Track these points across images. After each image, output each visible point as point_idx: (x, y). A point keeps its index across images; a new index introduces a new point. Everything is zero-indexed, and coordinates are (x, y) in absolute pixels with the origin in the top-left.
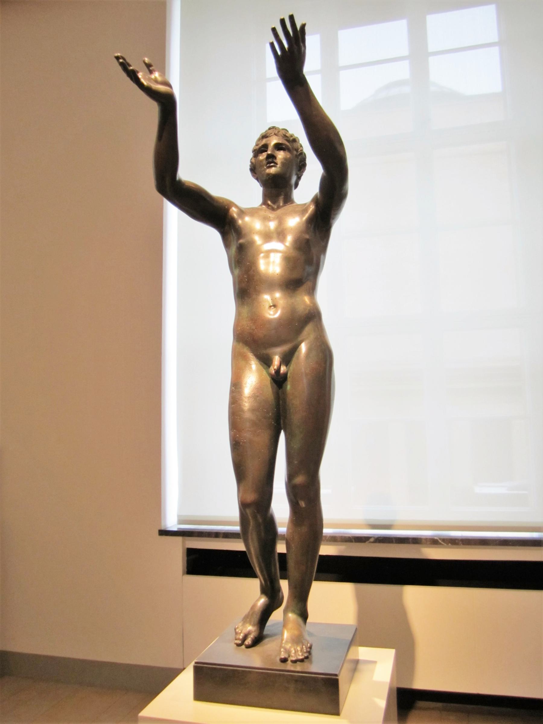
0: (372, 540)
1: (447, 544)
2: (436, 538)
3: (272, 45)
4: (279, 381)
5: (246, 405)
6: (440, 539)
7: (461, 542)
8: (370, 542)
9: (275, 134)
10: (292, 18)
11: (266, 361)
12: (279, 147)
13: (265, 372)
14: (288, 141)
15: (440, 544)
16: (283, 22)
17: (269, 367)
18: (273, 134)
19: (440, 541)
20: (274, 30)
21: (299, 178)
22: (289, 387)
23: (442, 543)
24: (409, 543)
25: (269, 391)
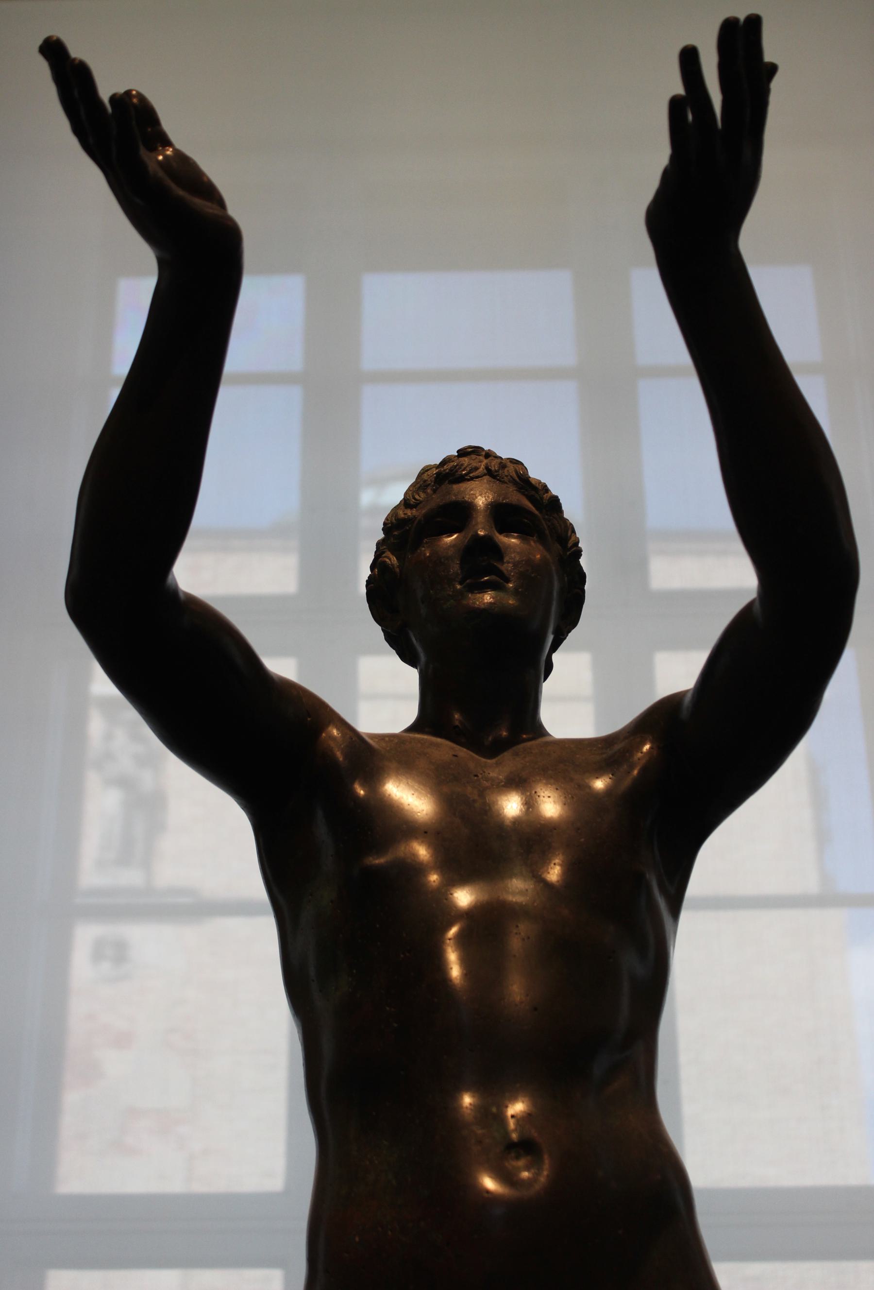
3: (676, 106)
9: (489, 472)
10: (754, 23)
12: (504, 516)
20: (689, 59)
21: (555, 647)
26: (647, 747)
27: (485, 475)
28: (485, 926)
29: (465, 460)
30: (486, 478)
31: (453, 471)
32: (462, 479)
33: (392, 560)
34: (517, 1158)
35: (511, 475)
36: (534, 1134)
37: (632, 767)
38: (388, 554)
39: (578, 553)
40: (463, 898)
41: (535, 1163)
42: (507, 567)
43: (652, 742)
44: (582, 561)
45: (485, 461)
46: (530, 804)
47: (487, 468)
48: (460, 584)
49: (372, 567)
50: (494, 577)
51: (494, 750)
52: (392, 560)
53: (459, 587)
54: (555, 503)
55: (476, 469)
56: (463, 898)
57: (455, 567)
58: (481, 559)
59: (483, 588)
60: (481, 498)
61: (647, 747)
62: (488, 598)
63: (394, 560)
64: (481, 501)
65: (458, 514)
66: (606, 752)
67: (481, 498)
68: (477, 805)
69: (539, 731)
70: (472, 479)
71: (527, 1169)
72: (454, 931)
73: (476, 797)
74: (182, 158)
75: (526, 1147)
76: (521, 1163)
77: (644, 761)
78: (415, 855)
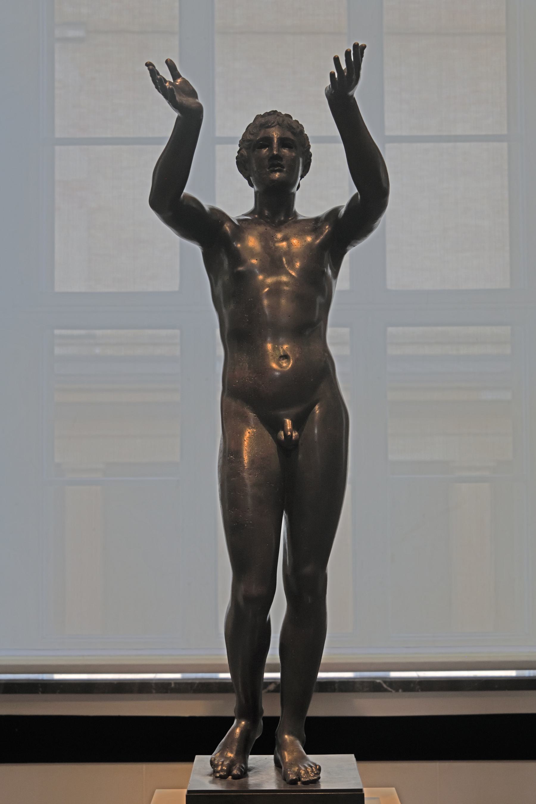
0: (272, 687)
1: (397, 691)
2: (378, 681)
3: (332, 75)
4: (287, 449)
5: (248, 477)
6: (385, 682)
7: (418, 687)
8: (269, 691)
9: (278, 124)
11: (273, 425)
12: (284, 143)
13: (269, 438)
14: (294, 133)
15: (385, 690)
16: (348, 53)
17: (278, 431)
19: (385, 686)
20: (336, 60)
22: (300, 456)
23: (389, 689)
24: (333, 690)
26: (327, 227)
28: (276, 291)
30: (277, 126)
31: (266, 123)
32: (269, 127)
33: (244, 152)
36: (288, 353)
37: (322, 234)
38: (243, 150)
40: (269, 280)
41: (289, 361)
42: (284, 162)
43: (329, 226)
44: (311, 150)
45: (278, 118)
46: (290, 245)
48: (268, 169)
49: (238, 152)
50: (280, 168)
51: (279, 226)
52: (244, 152)
53: (268, 170)
55: (273, 123)
56: (269, 280)
57: (266, 162)
58: (275, 162)
59: (276, 171)
60: (275, 134)
62: (277, 175)
63: (245, 152)
64: (275, 136)
65: (267, 142)
66: (315, 225)
67: (275, 134)
68: (273, 248)
69: (295, 214)
70: (272, 127)
71: (285, 363)
72: (266, 290)
73: (272, 246)
74: (185, 82)
75: (285, 357)
76: (284, 361)
78: (252, 264)
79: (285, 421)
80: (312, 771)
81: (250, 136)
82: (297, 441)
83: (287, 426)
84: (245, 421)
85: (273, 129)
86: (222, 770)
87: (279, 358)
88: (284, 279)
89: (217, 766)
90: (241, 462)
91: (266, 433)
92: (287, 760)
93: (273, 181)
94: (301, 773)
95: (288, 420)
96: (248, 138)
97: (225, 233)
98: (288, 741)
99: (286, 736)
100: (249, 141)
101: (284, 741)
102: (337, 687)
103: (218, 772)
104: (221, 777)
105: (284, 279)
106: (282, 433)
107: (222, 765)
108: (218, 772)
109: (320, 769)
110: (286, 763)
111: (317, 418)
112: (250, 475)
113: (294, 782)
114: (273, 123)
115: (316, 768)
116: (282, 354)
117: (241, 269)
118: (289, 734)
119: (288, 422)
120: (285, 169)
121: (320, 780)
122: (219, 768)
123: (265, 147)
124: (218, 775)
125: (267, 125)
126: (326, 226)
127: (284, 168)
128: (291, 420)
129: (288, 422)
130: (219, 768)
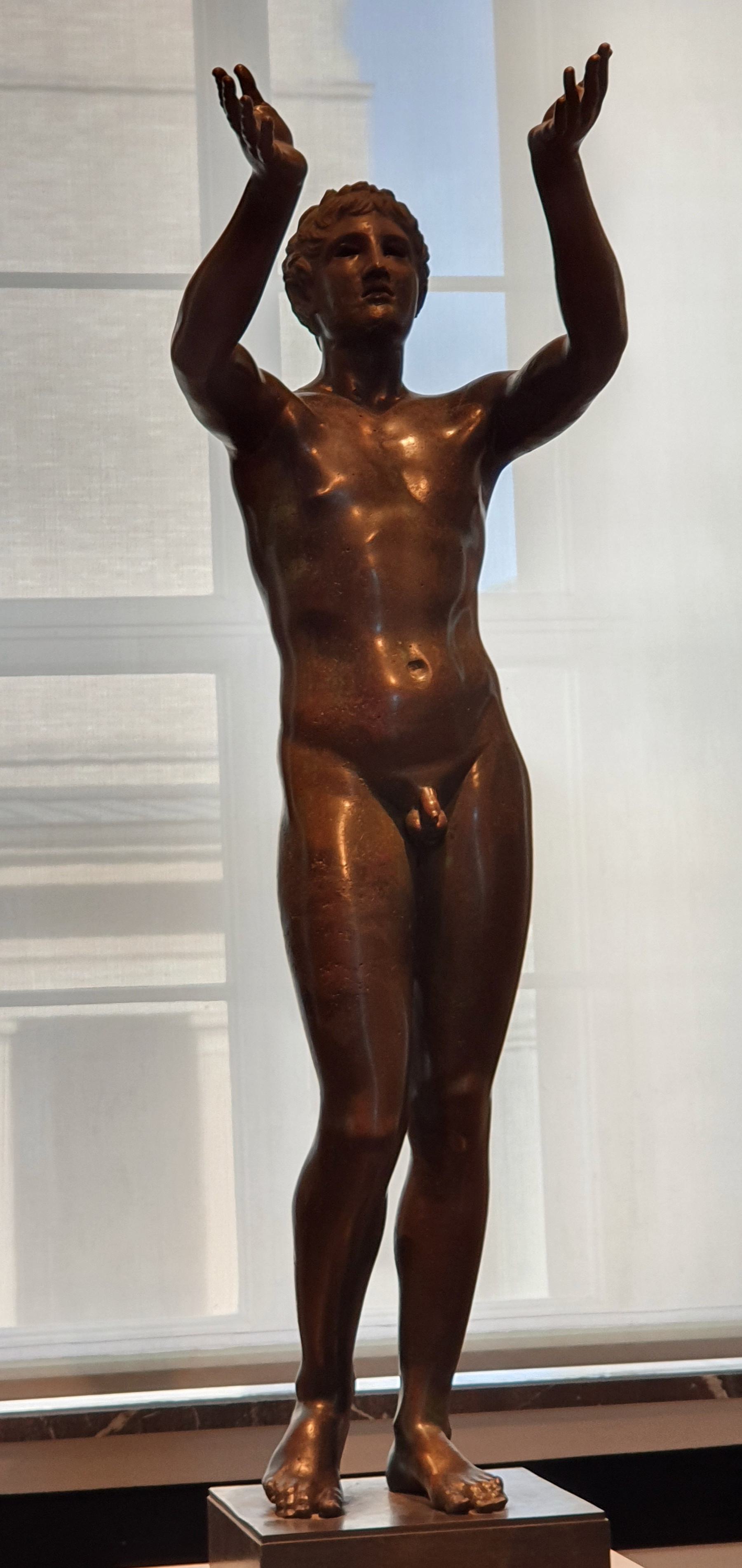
0: (118, 1423)
4: (424, 845)
8: (112, 1433)
9: (376, 207)
11: (398, 799)
18: (371, 205)
20: (569, 75)
22: (449, 861)
24: (248, 1423)
25: (402, 872)
26: (479, 411)
27: (373, 209)
29: (357, 194)
30: (374, 212)
31: (352, 205)
32: (358, 213)
34: (414, 670)
35: (385, 205)
36: (423, 657)
38: (302, 259)
39: (427, 259)
42: (391, 285)
44: (429, 263)
47: (374, 204)
50: (386, 294)
51: (383, 409)
52: (305, 263)
53: (361, 299)
54: (415, 224)
55: (366, 206)
56: (378, 516)
59: (377, 302)
61: (479, 411)
63: (308, 264)
75: (418, 664)
77: (478, 420)
79: (422, 792)
80: (491, 1488)
81: (318, 231)
82: (444, 829)
83: (427, 800)
84: (341, 790)
85: (364, 218)
86: (299, 1502)
87: (401, 667)
88: (405, 511)
89: (286, 1495)
90: (339, 873)
91: (382, 814)
92: (435, 1472)
93: (375, 321)
94: (472, 1493)
95: (426, 789)
96: (315, 236)
97: (288, 421)
98: (426, 1435)
99: (420, 1426)
100: (314, 241)
101: (418, 1435)
102: (254, 1416)
103: (289, 1507)
104: (299, 1515)
105: (405, 511)
106: (416, 813)
107: (295, 1492)
108: (289, 1507)
109: (501, 1484)
110: (436, 1475)
111: (477, 784)
112: (361, 896)
113: (463, 1509)
114: (366, 206)
115: (496, 1483)
116: (413, 658)
117: (321, 492)
118: (425, 1421)
119: (429, 792)
120: (394, 298)
121: (508, 1505)
122: (291, 1500)
123: (351, 253)
124: (290, 1513)
125: (354, 210)
126: (476, 409)
127: (392, 294)
128: (434, 788)
129: (429, 792)
130: (291, 1500)
